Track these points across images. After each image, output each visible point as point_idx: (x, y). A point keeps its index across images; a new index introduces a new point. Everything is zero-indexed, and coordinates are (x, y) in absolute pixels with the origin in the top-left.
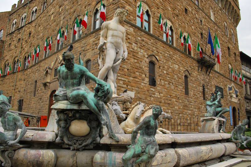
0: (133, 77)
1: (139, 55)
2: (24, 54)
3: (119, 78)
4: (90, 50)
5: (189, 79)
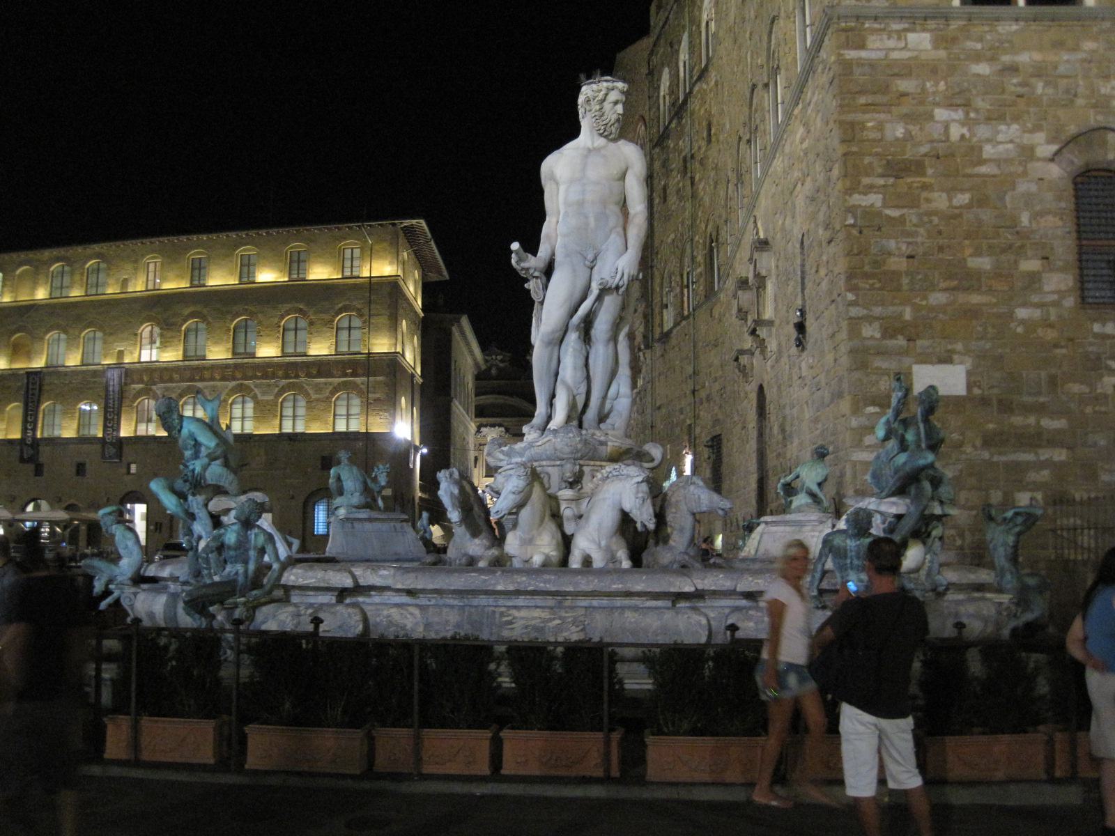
0: (946, 290)
2: (703, 226)
4: (799, 185)
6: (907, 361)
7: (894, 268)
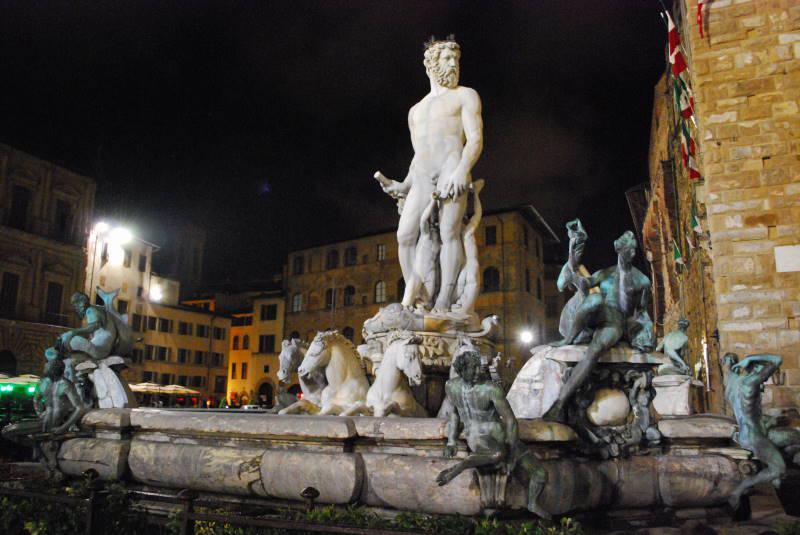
3: (717, 208)
6: (768, 244)
7: (751, 168)
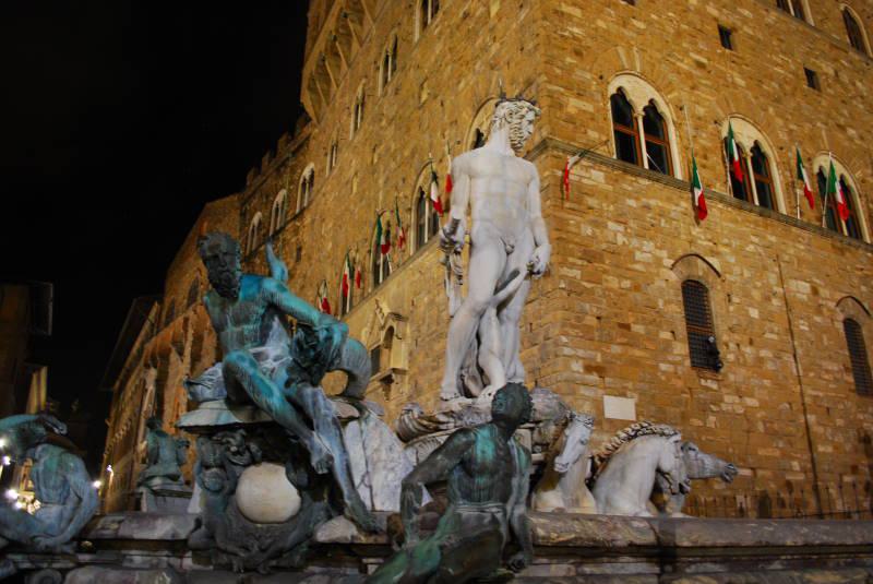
1: (639, 262)
3: (567, 351)
5: (864, 332)
6: (600, 392)
7: (588, 323)
